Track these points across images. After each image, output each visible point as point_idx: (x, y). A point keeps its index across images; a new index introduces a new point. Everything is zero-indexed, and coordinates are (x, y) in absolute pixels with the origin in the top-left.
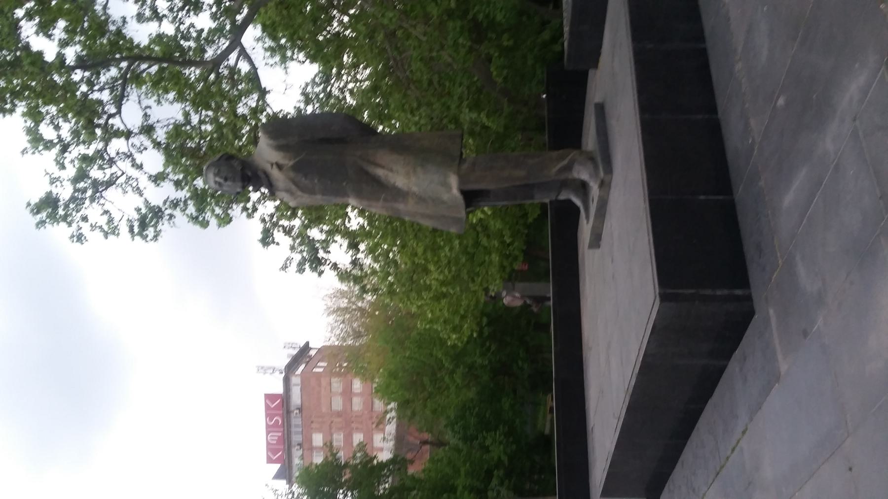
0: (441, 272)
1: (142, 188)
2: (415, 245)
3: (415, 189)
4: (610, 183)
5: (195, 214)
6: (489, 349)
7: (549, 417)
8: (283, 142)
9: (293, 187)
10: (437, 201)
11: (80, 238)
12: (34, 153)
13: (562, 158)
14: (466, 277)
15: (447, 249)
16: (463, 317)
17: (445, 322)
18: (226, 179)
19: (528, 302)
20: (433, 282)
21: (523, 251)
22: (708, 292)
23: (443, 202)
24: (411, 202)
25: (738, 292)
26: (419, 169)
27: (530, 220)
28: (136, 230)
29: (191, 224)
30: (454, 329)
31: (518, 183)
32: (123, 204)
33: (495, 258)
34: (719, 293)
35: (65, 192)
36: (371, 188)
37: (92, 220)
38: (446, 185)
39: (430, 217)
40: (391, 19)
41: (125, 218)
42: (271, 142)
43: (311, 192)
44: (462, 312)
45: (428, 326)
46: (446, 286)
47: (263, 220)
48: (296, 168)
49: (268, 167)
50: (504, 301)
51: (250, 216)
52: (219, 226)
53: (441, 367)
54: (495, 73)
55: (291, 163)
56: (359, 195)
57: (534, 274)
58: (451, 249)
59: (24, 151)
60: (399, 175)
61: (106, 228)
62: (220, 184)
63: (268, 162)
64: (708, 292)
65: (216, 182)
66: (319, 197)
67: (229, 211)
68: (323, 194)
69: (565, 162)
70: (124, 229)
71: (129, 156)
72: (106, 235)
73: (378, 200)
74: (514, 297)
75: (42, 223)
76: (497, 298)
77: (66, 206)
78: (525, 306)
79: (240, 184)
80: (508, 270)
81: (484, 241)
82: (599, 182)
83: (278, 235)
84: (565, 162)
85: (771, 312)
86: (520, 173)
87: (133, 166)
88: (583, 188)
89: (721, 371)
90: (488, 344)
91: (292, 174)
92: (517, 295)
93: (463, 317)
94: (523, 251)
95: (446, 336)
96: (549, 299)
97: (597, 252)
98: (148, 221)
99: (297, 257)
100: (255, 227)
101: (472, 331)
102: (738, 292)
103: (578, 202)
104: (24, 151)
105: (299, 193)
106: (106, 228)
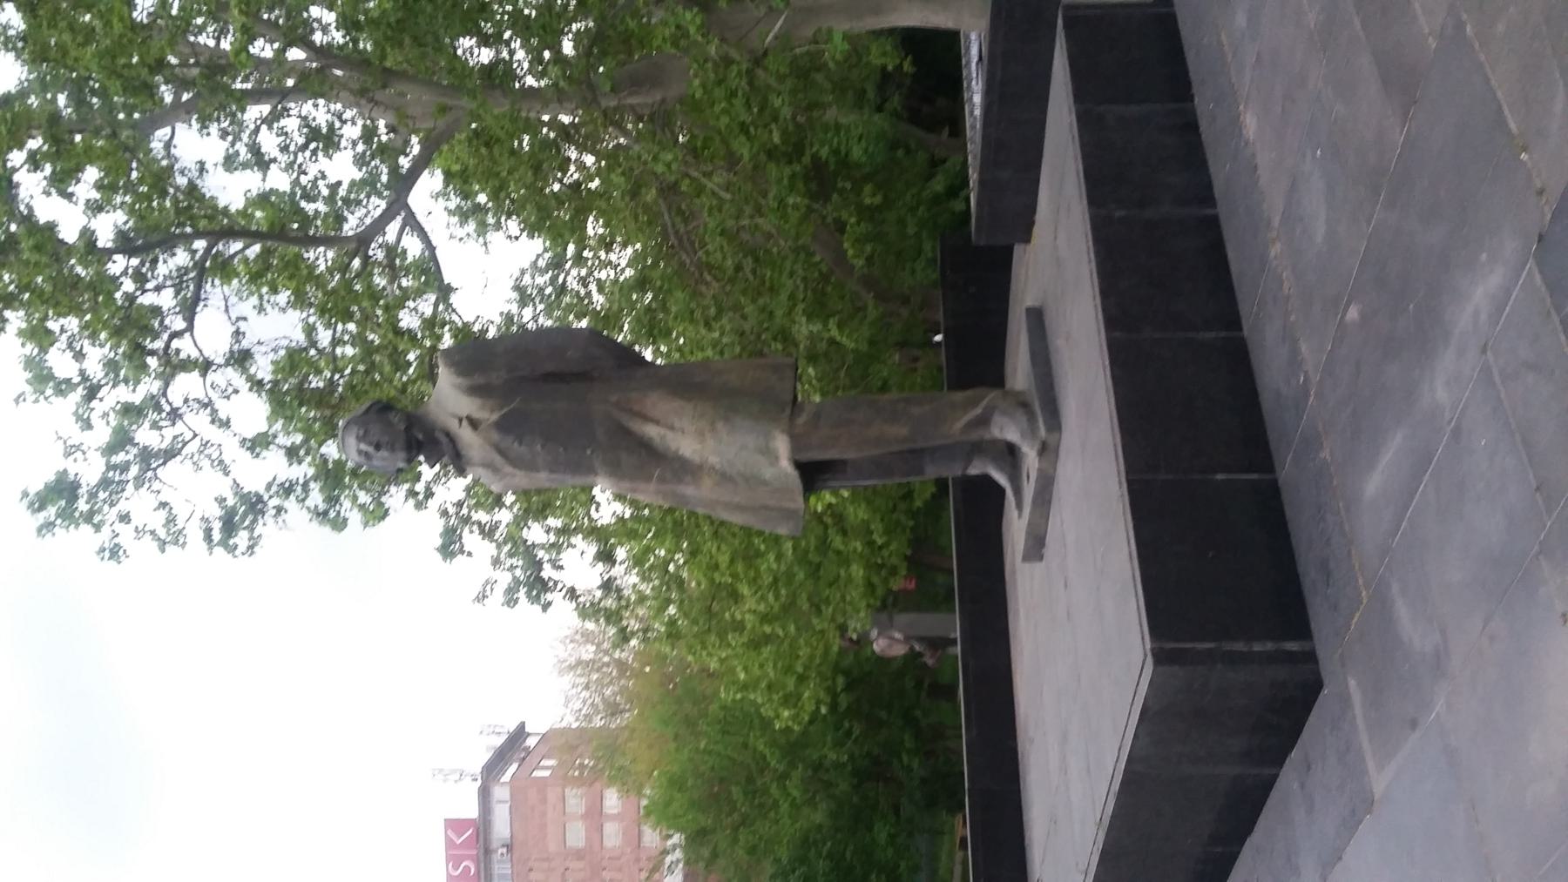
0: (763, 598)
1: (227, 462)
2: (714, 550)
3: (714, 460)
5: (322, 507)
6: (849, 733)
7: (959, 855)
8: (479, 380)
9: (498, 459)
10: (752, 481)
11: (115, 552)
12: (37, 401)
13: (974, 403)
14: (806, 607)
15: (772, 557)
16: (802, 679)
17: (769, 687)
18: (378, 447)
19: (917, 648)
20: (747, 616)
21: (906, 558)
22: (1240, 646)
23: (765, 483)
24: (707, 482)
25: (1292, 646)
26: (720, 425)
27: (918, 503)
28: (216, 536)
29: (315, 524)
30: (787, 701)
31: (895, 448)
32: (193, 490)
33: (857, 571)
34: (1257, 647)
35: (90, 471)
36: (637, 459)
37: (137, 520)
38: (769, 454)
39: (739, 508)
40: (668, 165)
41: (197, 515)
42: (459, 380)
43: (528, 466)
44: (800, 669)
45: (739, 696)
46: (770, 622)
47: (445, 513)
48: (502, 426)
49: (453, 425)
50: (875, 646)
51: (419, 506)
52: (366, 525)
53: (763, 766)
54: (850, 252)
55: (495, 417)
56: (616, 471)
57: (927, 598)
58: (779, 557)
59: (19, 399)
60: (684, 434)
61: (162, 533)
62: (367, 455)
63: (454, 416)
64: (1240, 646)
65: (360, 452)
67: (383, 499)
68: (552, 471)
69: (978, 411)
70: (195, 534)
71: (207, 405)
72: (163, 545)
73: (649, 479)
74: (892, 638)
75: (49, 526)
76: (863, 641)
77: (92, 495)
78: (913, 656)
79: (402, 455)
80: (880, 591)
81: (837, 542)
82: (1037, 446)
83: (471, 539)
84: (978, 411)
85: (1352, 683)
86: (902, 431)
87: (213, 422)
88: (1010, 455)
89: (1268, 785)
90: (847, 725)
91: (495, 436)
92: (898, 635)
93: (802, 679)
94: (906, 558)
95: (771, 714)
96: (954, 642)
97: (1038, 568)
98: (240, 518)
99: (504, 579)
100: (431, 525)
101: (818, 703)
102: (1292, 646)
103: (1001, 479)
104: (19, 399)
105: (509, 469)
106: (162, 533)
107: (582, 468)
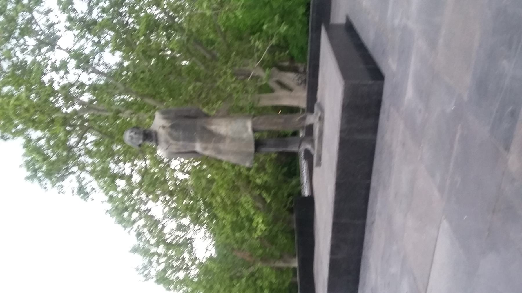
4: (323, 119)
10: (241, 139)
23: (244, 140)
39: (235, 153)
48: (172, 127)
55: (170, 124)
60: (222, 127)
66: (181, 143)
79: (142, 136)
91: (169, 130)
107: (192, 140)
